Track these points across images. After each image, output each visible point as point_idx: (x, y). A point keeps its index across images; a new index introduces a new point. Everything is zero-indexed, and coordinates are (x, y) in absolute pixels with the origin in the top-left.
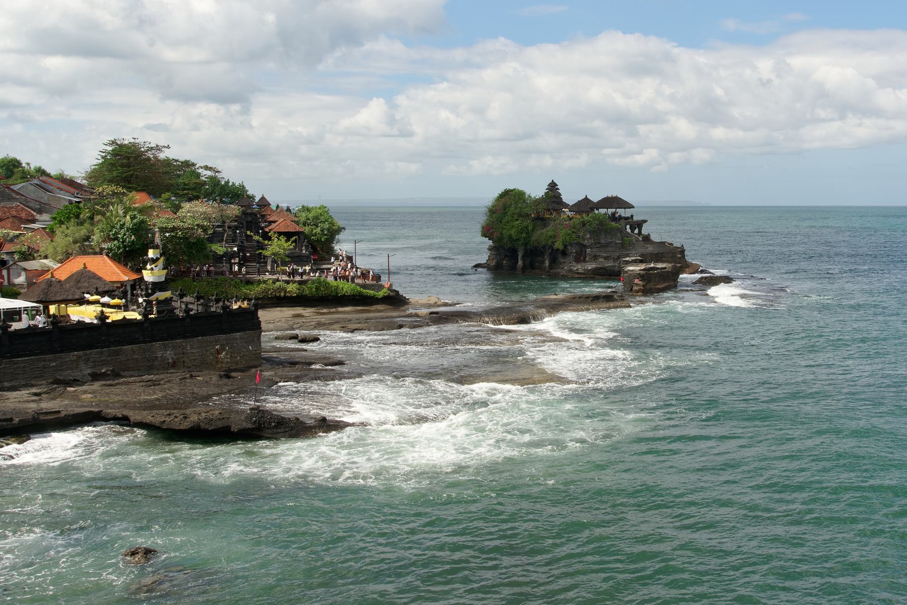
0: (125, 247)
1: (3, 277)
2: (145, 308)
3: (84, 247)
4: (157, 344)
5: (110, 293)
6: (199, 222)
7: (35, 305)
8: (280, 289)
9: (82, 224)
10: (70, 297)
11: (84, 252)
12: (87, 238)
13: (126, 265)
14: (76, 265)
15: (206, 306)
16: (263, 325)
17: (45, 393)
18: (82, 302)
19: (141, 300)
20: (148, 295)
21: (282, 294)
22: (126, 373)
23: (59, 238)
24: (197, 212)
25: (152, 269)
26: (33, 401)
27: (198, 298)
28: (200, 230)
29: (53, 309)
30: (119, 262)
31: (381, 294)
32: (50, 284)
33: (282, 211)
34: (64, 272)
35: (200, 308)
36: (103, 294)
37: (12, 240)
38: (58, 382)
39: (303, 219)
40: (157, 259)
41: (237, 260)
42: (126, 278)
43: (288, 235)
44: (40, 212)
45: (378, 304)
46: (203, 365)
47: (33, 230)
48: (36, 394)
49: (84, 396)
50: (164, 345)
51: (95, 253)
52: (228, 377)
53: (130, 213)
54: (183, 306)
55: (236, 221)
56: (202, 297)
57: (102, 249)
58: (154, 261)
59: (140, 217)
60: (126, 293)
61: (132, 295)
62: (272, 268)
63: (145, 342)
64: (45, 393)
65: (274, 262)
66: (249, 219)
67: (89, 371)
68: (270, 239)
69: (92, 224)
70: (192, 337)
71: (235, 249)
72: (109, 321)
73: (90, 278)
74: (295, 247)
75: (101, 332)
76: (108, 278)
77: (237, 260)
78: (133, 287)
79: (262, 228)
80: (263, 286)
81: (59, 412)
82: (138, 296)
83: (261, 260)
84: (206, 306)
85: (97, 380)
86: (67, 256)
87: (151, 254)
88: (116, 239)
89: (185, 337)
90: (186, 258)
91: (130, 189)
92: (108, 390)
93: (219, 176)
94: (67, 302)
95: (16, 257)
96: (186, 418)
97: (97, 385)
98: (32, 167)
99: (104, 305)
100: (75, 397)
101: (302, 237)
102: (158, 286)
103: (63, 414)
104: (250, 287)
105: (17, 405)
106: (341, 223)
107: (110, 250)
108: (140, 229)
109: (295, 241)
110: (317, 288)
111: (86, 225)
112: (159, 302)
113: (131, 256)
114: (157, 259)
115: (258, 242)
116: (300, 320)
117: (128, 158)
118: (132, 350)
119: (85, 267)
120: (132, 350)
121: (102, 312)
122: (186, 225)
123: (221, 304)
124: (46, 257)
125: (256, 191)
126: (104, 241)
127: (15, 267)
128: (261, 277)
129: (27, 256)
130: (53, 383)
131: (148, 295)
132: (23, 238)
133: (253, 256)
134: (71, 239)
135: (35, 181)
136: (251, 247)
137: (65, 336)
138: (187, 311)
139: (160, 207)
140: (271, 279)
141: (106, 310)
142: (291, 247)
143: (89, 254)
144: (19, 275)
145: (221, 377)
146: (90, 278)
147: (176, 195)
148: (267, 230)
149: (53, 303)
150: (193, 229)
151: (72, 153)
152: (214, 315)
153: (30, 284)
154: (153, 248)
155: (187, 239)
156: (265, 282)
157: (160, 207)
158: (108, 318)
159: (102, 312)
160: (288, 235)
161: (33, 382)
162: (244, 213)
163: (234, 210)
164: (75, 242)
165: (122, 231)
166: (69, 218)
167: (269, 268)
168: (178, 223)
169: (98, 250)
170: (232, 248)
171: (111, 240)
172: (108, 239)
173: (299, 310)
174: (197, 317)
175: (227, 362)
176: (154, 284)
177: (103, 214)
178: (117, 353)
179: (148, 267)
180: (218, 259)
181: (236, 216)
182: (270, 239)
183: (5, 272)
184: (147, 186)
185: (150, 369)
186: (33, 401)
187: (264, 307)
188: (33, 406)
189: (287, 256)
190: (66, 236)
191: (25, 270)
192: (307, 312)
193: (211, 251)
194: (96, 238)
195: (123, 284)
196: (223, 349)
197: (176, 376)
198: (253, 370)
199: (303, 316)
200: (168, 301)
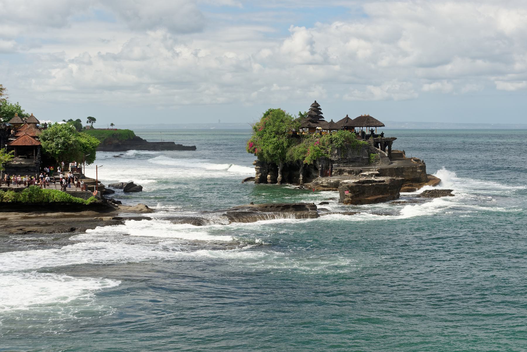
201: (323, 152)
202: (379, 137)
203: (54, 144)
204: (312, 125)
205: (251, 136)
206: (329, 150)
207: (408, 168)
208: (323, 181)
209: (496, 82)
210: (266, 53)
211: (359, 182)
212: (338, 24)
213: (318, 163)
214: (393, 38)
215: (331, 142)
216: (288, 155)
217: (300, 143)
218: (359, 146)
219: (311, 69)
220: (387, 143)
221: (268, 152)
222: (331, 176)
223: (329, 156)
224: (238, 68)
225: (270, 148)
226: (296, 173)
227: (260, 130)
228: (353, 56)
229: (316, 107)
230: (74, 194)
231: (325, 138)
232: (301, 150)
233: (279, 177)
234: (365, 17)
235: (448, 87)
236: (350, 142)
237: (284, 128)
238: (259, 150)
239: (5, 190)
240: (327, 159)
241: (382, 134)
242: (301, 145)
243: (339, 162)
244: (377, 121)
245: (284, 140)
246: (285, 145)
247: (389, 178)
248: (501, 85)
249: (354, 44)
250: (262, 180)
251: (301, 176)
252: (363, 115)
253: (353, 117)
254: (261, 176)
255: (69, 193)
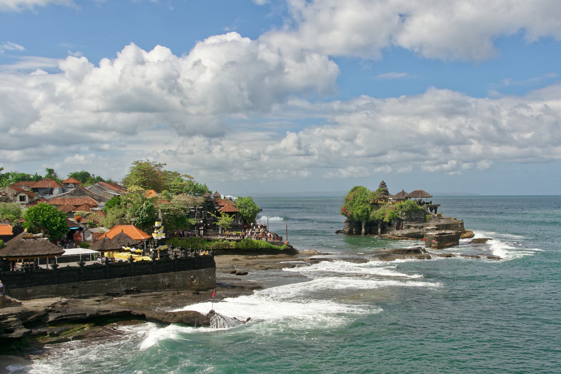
0: (143, 220)
1: (81, 237)
2: (154, 255)
3: (122, 220)
4: (160, 275)
5: (135, 246)
6: (182, 206)
7: (97, 252)
8: (226, 244)
9: (121, 208)
10: (115, 248)
11: (122, 223)
12: (123, 216)
13: (143, 230)
14: (118, 230)
15: (186, 253)
16: (217, 265)
17: (102, 300)
18: (121, 250)
19: (151, 250)
20: (155, 247)
21: (227, 247)
22: (144, 290)
23: (109, 216)
24: (181, 201)
25: (157, 233)
26: (96, 304)
27: (182, 249)
28: (182, 211)
29: (106, 254)
30: (140, 229)
31: (282, 248)
32: (104, 241)
33: (227, 200)
34: (111, 234)
35: (183, 255)
36: (131, 246)
37: (85, 217)
38: (108, 294)
39: (238, 204)
40: (160, 227)
41: (202, 228)
42: (144, 238)
43: (231, 214)
44: (100, 201)
45: (280, 253)
46: (184, 287)
47: (96, 211)
48: (98, 301)
49: (122, 303)
50: (164, 275)
51: (128, 224)
52: (198, 294)
53: (145, 202)
54: (174, 254)
55: (201, 206)
56: (184, 249)
57: (131, 222)
58: (158, 228)
59: (151, 204)
60: (144, 246)
61: (147, 247)
62: (222, 232)
63: (153, 273)
64: (102, 300)
65: (223, 229)
66: (209, 205)
67: (125, 289)
68: (220, 216)
69: (126, 208)
70: (179, 271)
71: (202, 222)
72: (135, 261)
73: (125, 237)
74: (234, 221)
75: (129, 268)
76: (134, 238)
77: (202, 228)
78: (147, 243)
79: (216, 210)
80: (216, 242)
81: (109, 311)
82: (150, 247)
83: (215, 228)
84: (186, 253)
85: (129, 294)
86: (113, 225)
87: (157, 224)
88: (138, 216)
89: (175, 271)
90: (175, 227)
91: (146, 189)
92: (134, 299)
93: (193, 180)
94: (113, 250)
95: (88, 226)
96: (175, 316)
97: (129, 297)
98: (96, 176)
99: (132, 253)
100: (117, 303)
101: (238, 215)
102: (161, 242)
103: (111, 312)
104: (209, 243)
105: (88, 306)
106: (258, 207)
107: (135, 222)
108: (151, 210)
109: (234, 217)
110: (246, 244)
111: (123, 208)
112: (161, 251)
113: (146, 225)
114: (160, 227)
115: (214, 217)
116: (237, 262)
117: (145, 171)
118: (147, 278)
119: (122, 232)
120: (147, 278)
121: (131, 256)
122: (175, 208)
123: (194, 253)
124: (102, 226)
125: (213, 189)
126: (132, 217)
127: (87, 231)
128: (215, 238)
129: (93, 225)
130: (106, 295)
131: (155, 247)
132: (90, 216)
133: (211, 226)
134: (115, 216)
135: (97, 184)
136: (210, 220)
137: (113, 270)
138: (176, 256)
139: (161, 198)
140: (220, 239)
141: (134, 255)
142: (232, 220)
143: (124, 224)
144: (89, 236)
145: (194, 293)
146: (125, 237)
147: (170, 191)
148: (219, 211)
149: (106, 251)
150: (178, 210)
151: (115, 169)
152: (190, 259)
153: (95, 241)
154: (158, 221)
155: (176, 216)
156: (218, 240)
157: (161, 198)
158: (134, 259)
159: (131, 256)
160: (231, 214)
161: (96, 294)
162: (206, 201)
163: (201, 200)
164: (117, 218)
165: (141, 212)
166: (114, 204)
167: (220, 232)
168: (171, 207)
169: (129, 222)
170: (200, 221)
171: (136, 216)
172: (134, 216)
173: (236, 257)
174: (181, 260)
175: (197, 286)
176: (158, 240)
177: (132, 202)
178: (139, 279)
179: (155, 231)
180: (192, 227)
181: (202, 203)
182: (220, 216)
183: (82, 234)
184: (154, 187)
185: (156, 289)
186: (96, 304)
187: (217, 254)
188: (96, 307)
189: (230, 226)
190: (113, 214)
191: (92, 233)
192: (241, 257)
193: (188, 223)
194: (128, 215)
195: (142, 241)
196: (194, 277)
197: (170, 293)
198: (212, 290)
199: (239, 260)
200: (165, 251)
201: (396, 214)
202: (430, 204)
203: (247, 211)
204: (386, 196)
205: (343, 205)
206: (400, 213)
207: (453, 224)
208: (399, 233)
209: (422, 166)
210: (270, 148)
211: (438, 234)
212: (318, 130)
213: (393, 221)
214: (351, 139)
215: (402, 207)
216: (371, 216)
217: (378, 208)
218: (418, 210)
219: (301, 159)
220: (435, 208)
221: (357, 214)
222: (402, 229)
223: (400, 217)
224: (252, 159)
225: (359, 212)
226: (375, 227)
227: (351, 201)
228: (328, 150)
229: (383, 184)
230: (273, 243)
231: (397, 205)
232: (381, 213)
233: (363, 230)
234: (336, 124)
235: (389, 169)
236: (413, 207)
237: (368, 199)
238: (350, 213)
239: (230, 240)
240: (399, 219)
241: (431, 202)
242: (380, 209)
243: (406, 220)
244: (427, 194)
245: (368, 206)
246: (369, 209)
247: (454, 232)
248: (425, 168)
249: (328, 142)
250: (350, 233)
251: (379, 229)
252: (418, 190)
253: (409, 191)
254: (349, 230)
255: (269, 242)
